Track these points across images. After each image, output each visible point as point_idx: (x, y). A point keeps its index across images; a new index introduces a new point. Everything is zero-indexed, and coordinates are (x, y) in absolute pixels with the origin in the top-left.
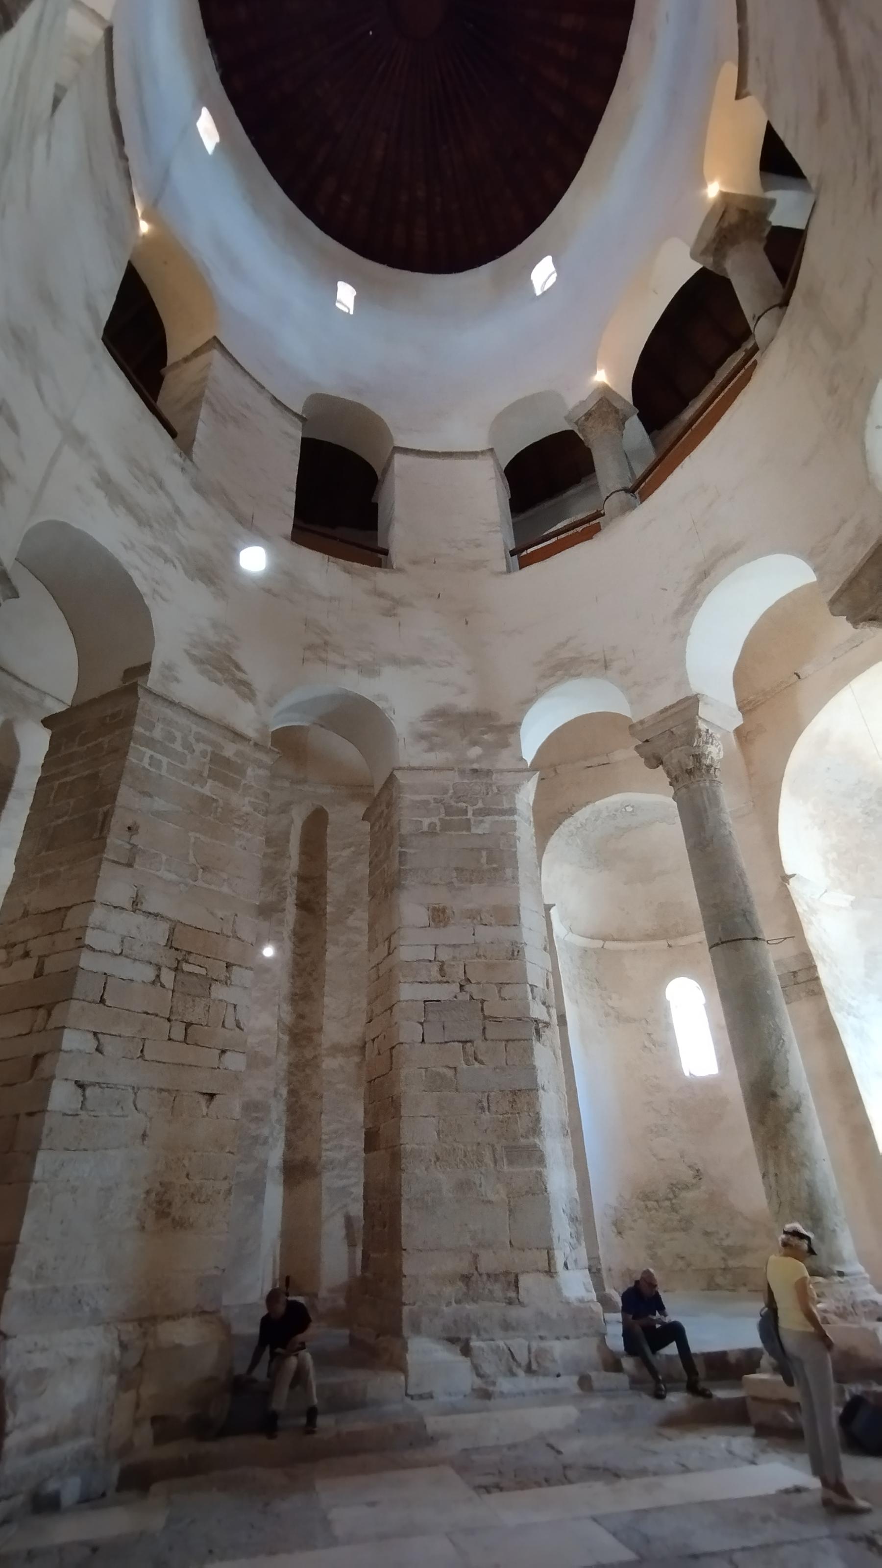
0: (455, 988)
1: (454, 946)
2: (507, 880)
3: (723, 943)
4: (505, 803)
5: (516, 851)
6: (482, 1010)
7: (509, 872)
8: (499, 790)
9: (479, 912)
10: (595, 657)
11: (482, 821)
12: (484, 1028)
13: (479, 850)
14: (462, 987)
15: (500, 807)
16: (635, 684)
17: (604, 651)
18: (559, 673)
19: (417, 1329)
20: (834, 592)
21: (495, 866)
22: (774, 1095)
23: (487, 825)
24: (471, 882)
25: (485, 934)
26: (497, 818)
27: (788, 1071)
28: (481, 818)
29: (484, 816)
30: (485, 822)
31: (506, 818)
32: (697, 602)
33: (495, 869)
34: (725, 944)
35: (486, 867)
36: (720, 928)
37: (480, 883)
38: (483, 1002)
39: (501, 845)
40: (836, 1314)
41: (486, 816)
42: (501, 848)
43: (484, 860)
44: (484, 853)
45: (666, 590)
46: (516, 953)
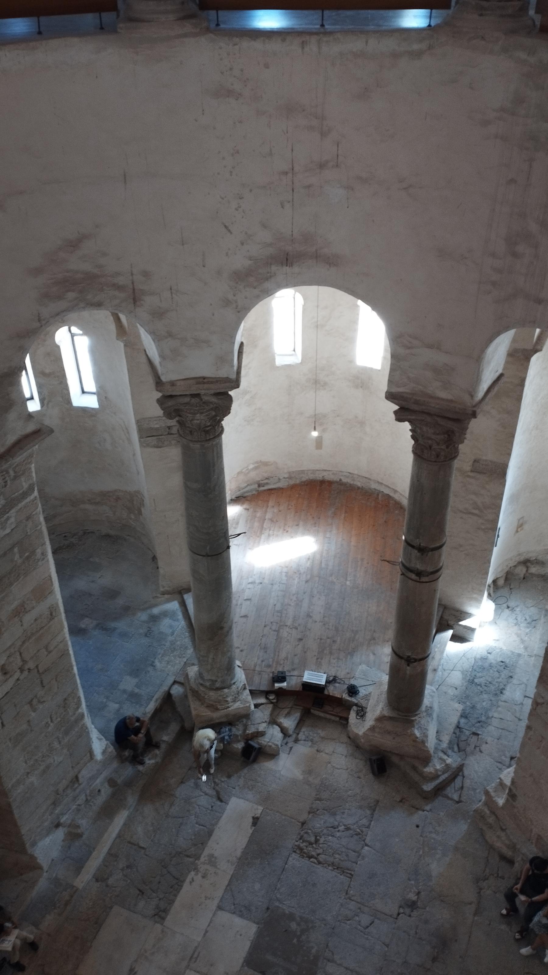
0: (17, 675)
1: (10, 647)
2: (39, 560)
3: (208, 556)
4: (24, 484)
5: (41, 528)
6: (38, 671)
7: (39, 551)
8: (15, 472)
9: (22, 605)
10: (121, 280)
11: (8, 519)
12: (42, 683)
13: (11, 549)
14: (22, 670)
15: (21, 492)
16: (170, 335)
17: (132, 274)
18: (71, 295)
19: (34, 844)
20: (401, 390)
21: (27, 554)
22: (222, 628)
23: (12, 520)
24: (11, 584)
25: (28, 618)
26: (20, 505)
27: (230, 613)
28: (5, 517)
29: (8, 513)
30: (11, 517)
31: (28, 500)
32: (267, 285)
33: (28, 558)
34: (209, 558)
35: (20, 561)
36: (208, 548)
37: (18, 580)
38: (37, 667)
39: (28, 530)
40: (232, 702)
41: (10, 510)
42: (29, 534)
43: (17, 557)
44: (16, 550)
45: (231, 233)
46: (54, 614)
